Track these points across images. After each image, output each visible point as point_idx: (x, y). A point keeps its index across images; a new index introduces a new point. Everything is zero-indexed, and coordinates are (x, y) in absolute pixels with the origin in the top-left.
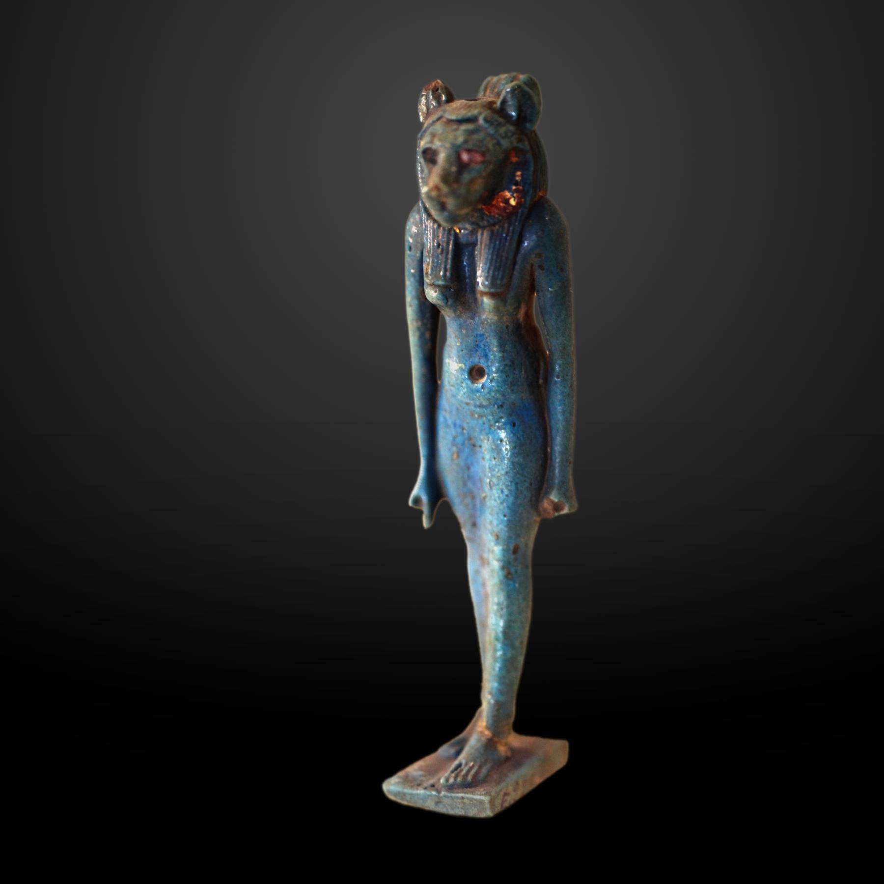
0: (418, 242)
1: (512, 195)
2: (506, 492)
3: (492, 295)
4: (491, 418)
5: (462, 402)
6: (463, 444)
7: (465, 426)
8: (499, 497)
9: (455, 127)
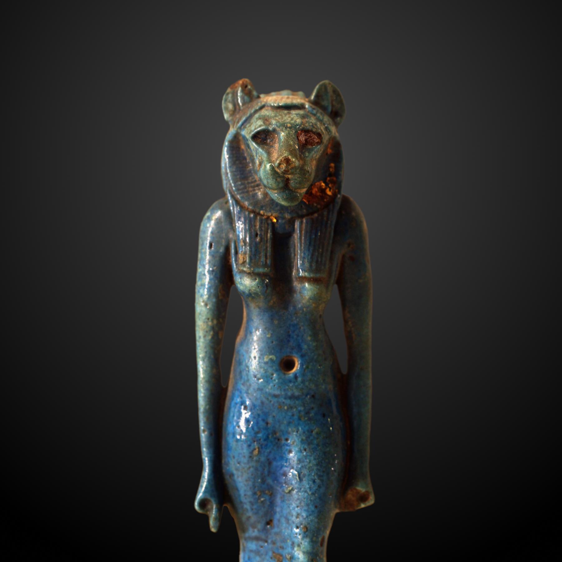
0: (221, 238)
1: (327, 185)
2: (318, 481)
3: (314, 281)
4: (302, 408)
5: (270, 394)
6: (266, 439)
7: (270, 420)
8: (310, 488)
9: (286, 112)
